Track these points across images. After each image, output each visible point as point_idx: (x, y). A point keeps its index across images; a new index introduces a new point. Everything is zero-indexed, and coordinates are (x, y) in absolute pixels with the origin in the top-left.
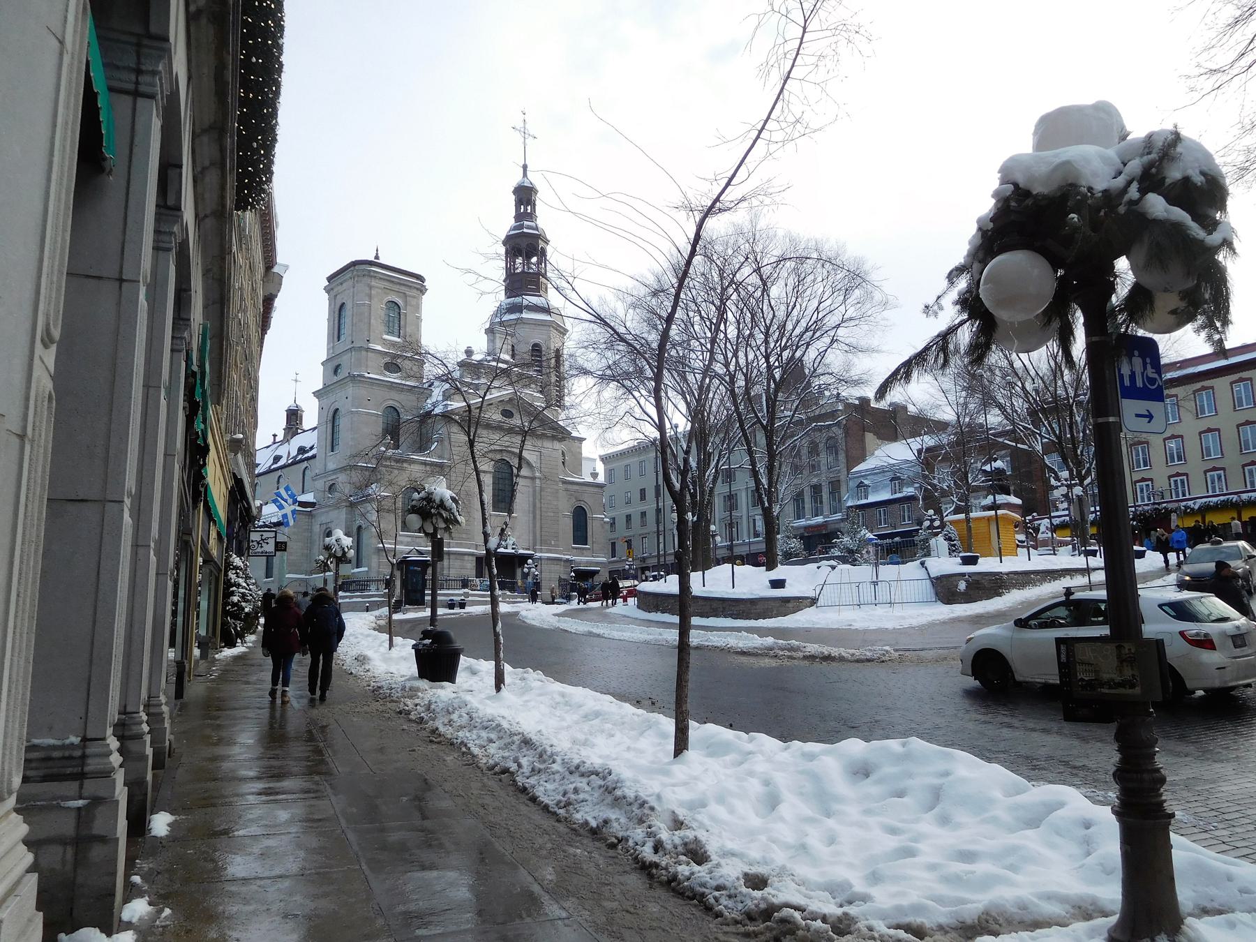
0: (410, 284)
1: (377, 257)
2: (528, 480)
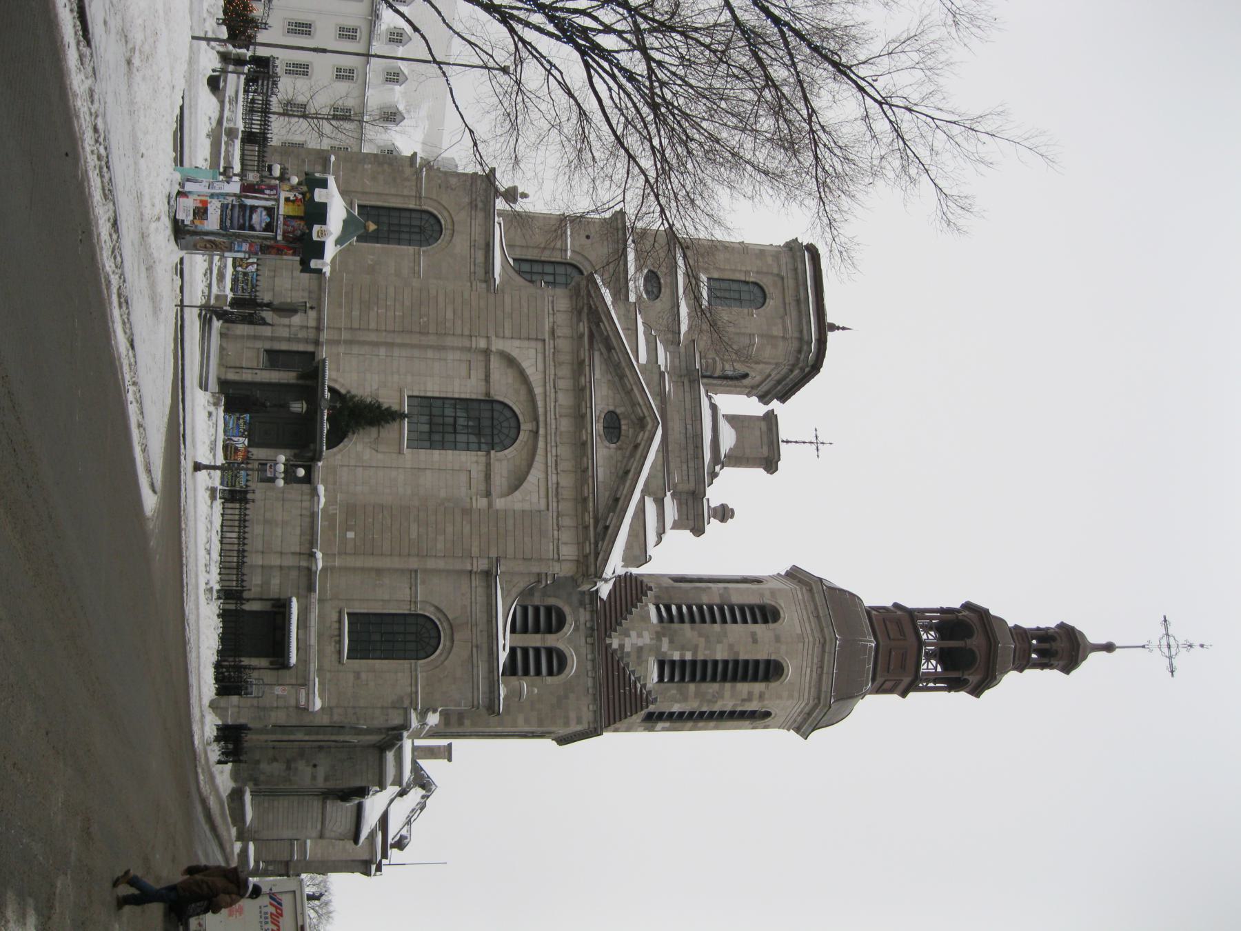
1: (833, 327)
2: (482, 487)
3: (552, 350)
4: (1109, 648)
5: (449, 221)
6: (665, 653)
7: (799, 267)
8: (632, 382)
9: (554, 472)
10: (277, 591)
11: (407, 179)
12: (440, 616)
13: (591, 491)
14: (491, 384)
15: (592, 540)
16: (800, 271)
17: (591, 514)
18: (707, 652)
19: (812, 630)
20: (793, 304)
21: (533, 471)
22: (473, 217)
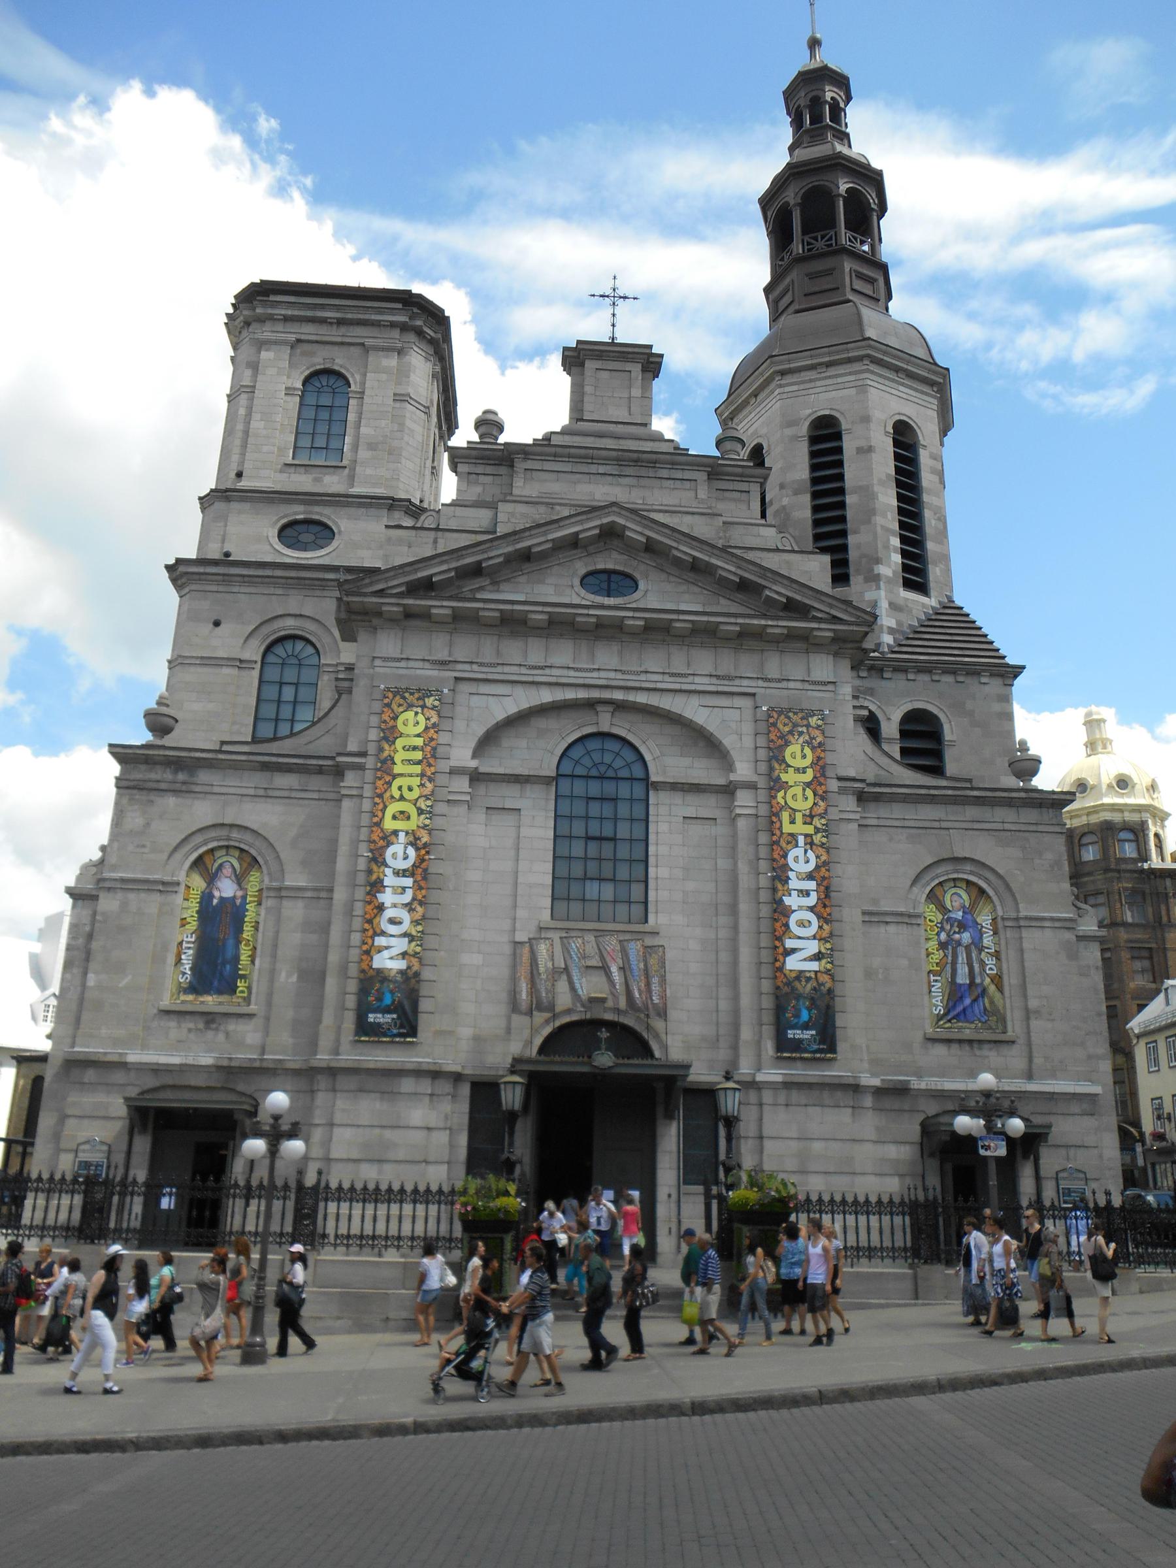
0: (373, 317)
3: (475, 667)
4: (814, 44)
5: (213, 834)
6: (894, 572)
7: (283, 312)
8: (542, 539)
9: (690, 679)
10: (908, 1147)
11: (124, 905)
12: (927, 877)
13: (732, 620)
14: (531, 773)
15: (814, 625)
16: (289, 312)
17: (770, 623)
18: (889, 516)
19: (850, 374)
20: (343, 330)
21: (688, 714)
22: (207, 789)
